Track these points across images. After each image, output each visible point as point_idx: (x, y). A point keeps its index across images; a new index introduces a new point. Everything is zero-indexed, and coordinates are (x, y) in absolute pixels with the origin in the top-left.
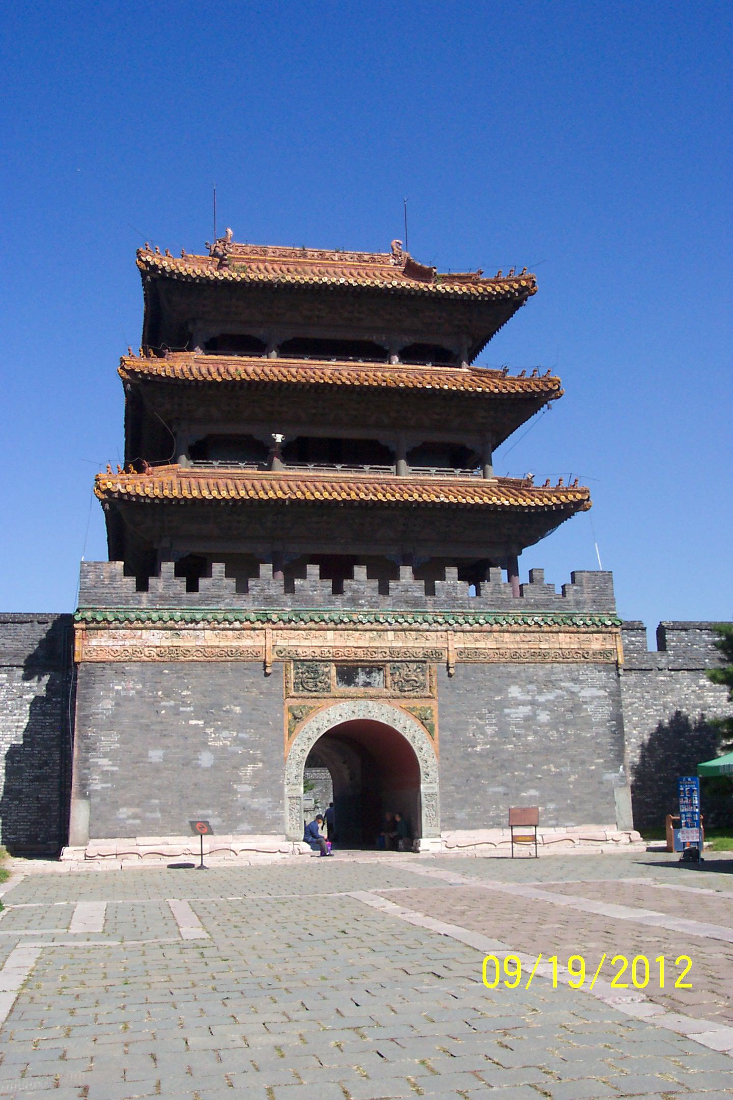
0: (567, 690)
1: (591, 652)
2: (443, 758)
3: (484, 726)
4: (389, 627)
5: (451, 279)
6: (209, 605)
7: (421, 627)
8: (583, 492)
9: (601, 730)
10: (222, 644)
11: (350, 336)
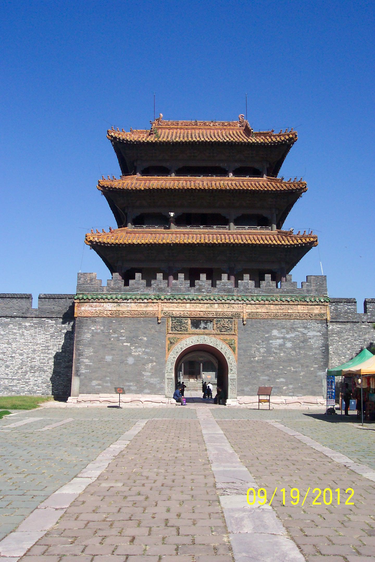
0: (301, 332)
1: (313, 315)
3: (259, 348)
4: (215, 302)
5: (260, 134)
6: (133, 292)
7: (230, 302)
8: (314, 238)
9: (317, 351)
10: (138, 309)
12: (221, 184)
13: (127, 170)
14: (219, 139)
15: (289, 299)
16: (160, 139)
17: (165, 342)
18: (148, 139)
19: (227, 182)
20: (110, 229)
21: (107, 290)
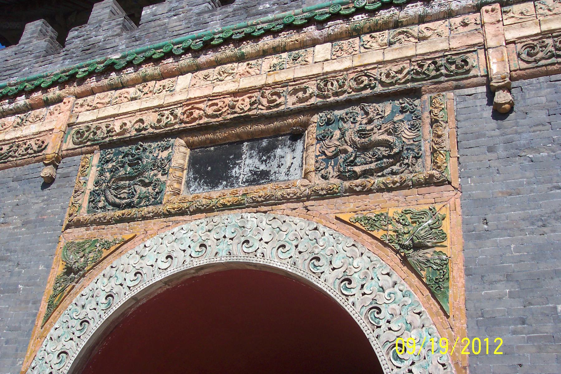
17: (48, 267)
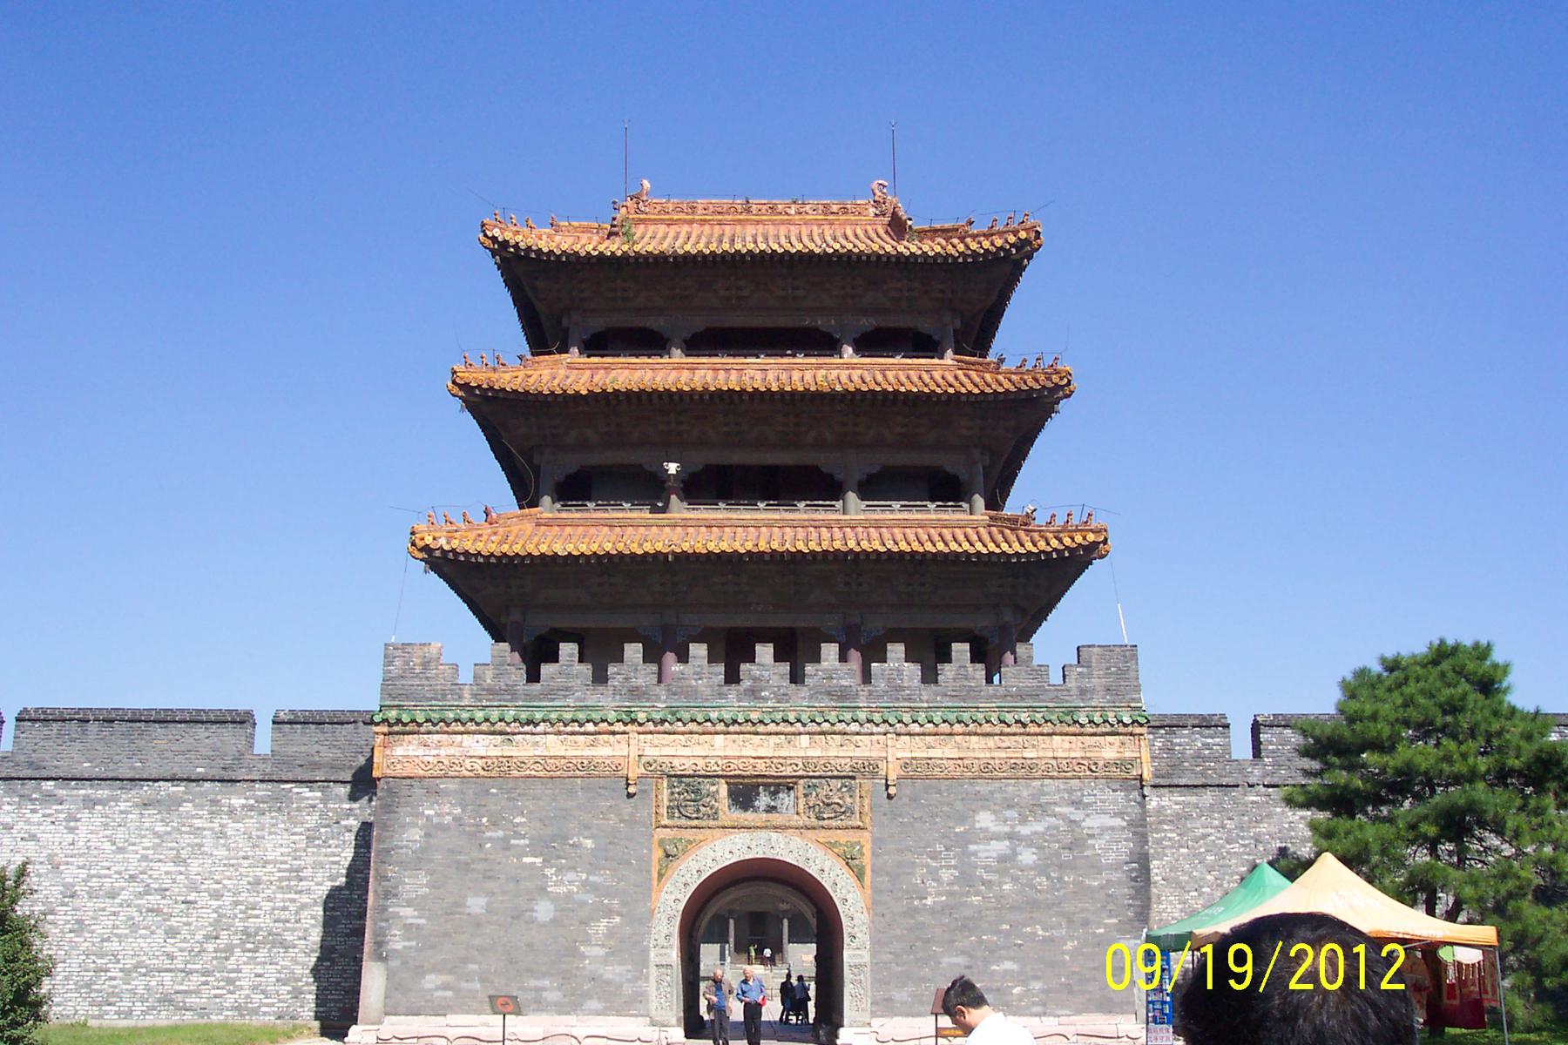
1: (1101, 763)
2: (876, 914)
7: (848, 729)
8: (1096, 532)
9: (1115, 876)
10: (568, 754)
11: (783, 321)
12: (819, 379)
13: (544, 335)
14: (812, 246)
15: (1024, 717)
16: (637, 248)
17: (650, 850)
18: (601, 248)
19: (835, 373)
20: (487, 513)
21: (474, 696)
